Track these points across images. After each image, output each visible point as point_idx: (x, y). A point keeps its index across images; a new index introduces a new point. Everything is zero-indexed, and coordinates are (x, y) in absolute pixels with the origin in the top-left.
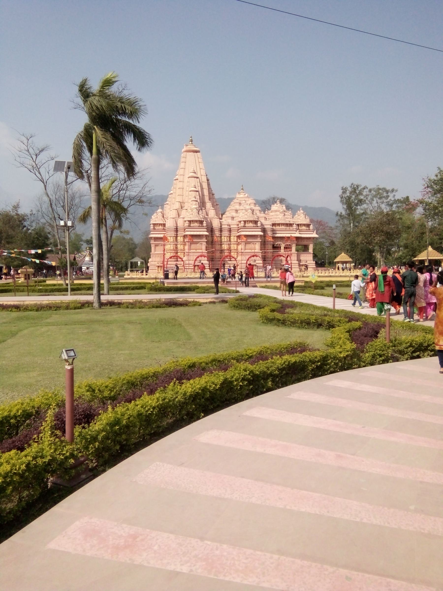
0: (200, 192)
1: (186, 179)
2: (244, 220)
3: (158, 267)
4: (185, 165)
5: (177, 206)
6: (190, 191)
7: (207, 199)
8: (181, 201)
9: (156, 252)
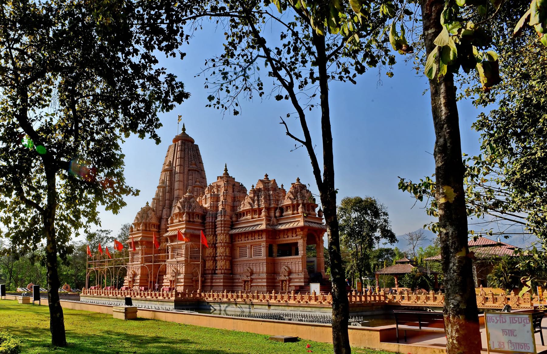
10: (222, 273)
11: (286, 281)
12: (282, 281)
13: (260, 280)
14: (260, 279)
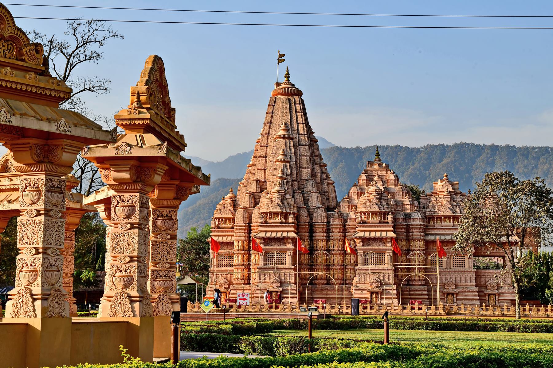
0: (294, 164)
1: (271, 144)
2: (363, 210)
5: (253, 188)
7: (306, 174)
8: (262, 178)
10: (420, 285)
11: (495, 295)
12: (489, 295)
13: (469, 294)
14: (469, 292)
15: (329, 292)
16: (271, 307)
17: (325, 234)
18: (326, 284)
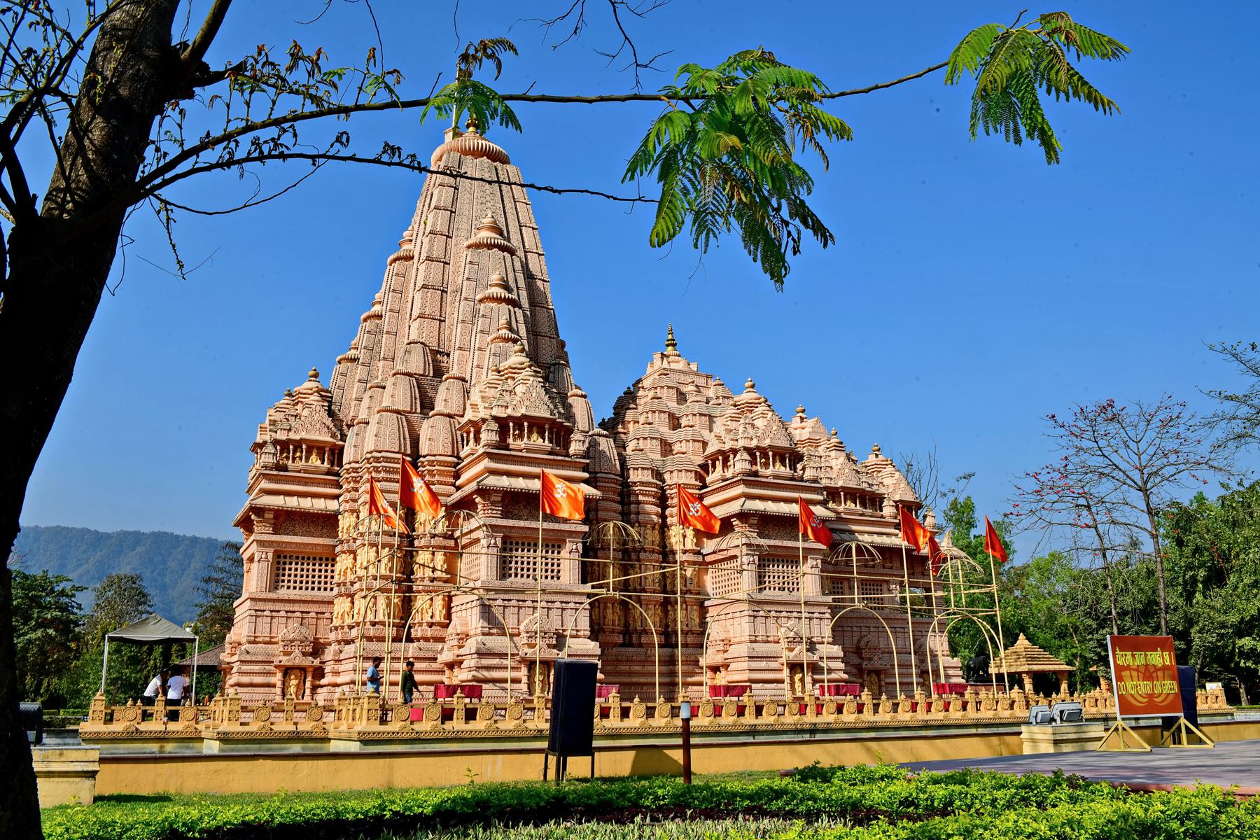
3: (287, 671)
4: (455, 199)
5: (416, 363)
6: (481, 301)
9: (283, 593)
15: (637, 668)
16: (447, 715)
17: (619, 507)
18: (623, 645)
